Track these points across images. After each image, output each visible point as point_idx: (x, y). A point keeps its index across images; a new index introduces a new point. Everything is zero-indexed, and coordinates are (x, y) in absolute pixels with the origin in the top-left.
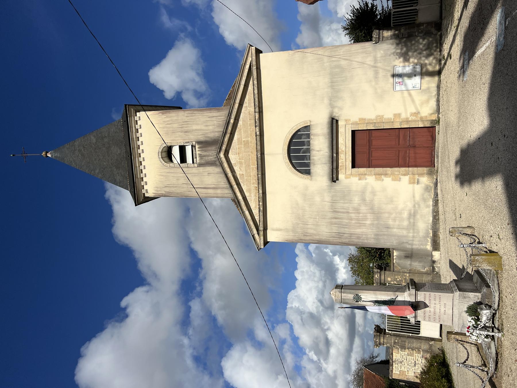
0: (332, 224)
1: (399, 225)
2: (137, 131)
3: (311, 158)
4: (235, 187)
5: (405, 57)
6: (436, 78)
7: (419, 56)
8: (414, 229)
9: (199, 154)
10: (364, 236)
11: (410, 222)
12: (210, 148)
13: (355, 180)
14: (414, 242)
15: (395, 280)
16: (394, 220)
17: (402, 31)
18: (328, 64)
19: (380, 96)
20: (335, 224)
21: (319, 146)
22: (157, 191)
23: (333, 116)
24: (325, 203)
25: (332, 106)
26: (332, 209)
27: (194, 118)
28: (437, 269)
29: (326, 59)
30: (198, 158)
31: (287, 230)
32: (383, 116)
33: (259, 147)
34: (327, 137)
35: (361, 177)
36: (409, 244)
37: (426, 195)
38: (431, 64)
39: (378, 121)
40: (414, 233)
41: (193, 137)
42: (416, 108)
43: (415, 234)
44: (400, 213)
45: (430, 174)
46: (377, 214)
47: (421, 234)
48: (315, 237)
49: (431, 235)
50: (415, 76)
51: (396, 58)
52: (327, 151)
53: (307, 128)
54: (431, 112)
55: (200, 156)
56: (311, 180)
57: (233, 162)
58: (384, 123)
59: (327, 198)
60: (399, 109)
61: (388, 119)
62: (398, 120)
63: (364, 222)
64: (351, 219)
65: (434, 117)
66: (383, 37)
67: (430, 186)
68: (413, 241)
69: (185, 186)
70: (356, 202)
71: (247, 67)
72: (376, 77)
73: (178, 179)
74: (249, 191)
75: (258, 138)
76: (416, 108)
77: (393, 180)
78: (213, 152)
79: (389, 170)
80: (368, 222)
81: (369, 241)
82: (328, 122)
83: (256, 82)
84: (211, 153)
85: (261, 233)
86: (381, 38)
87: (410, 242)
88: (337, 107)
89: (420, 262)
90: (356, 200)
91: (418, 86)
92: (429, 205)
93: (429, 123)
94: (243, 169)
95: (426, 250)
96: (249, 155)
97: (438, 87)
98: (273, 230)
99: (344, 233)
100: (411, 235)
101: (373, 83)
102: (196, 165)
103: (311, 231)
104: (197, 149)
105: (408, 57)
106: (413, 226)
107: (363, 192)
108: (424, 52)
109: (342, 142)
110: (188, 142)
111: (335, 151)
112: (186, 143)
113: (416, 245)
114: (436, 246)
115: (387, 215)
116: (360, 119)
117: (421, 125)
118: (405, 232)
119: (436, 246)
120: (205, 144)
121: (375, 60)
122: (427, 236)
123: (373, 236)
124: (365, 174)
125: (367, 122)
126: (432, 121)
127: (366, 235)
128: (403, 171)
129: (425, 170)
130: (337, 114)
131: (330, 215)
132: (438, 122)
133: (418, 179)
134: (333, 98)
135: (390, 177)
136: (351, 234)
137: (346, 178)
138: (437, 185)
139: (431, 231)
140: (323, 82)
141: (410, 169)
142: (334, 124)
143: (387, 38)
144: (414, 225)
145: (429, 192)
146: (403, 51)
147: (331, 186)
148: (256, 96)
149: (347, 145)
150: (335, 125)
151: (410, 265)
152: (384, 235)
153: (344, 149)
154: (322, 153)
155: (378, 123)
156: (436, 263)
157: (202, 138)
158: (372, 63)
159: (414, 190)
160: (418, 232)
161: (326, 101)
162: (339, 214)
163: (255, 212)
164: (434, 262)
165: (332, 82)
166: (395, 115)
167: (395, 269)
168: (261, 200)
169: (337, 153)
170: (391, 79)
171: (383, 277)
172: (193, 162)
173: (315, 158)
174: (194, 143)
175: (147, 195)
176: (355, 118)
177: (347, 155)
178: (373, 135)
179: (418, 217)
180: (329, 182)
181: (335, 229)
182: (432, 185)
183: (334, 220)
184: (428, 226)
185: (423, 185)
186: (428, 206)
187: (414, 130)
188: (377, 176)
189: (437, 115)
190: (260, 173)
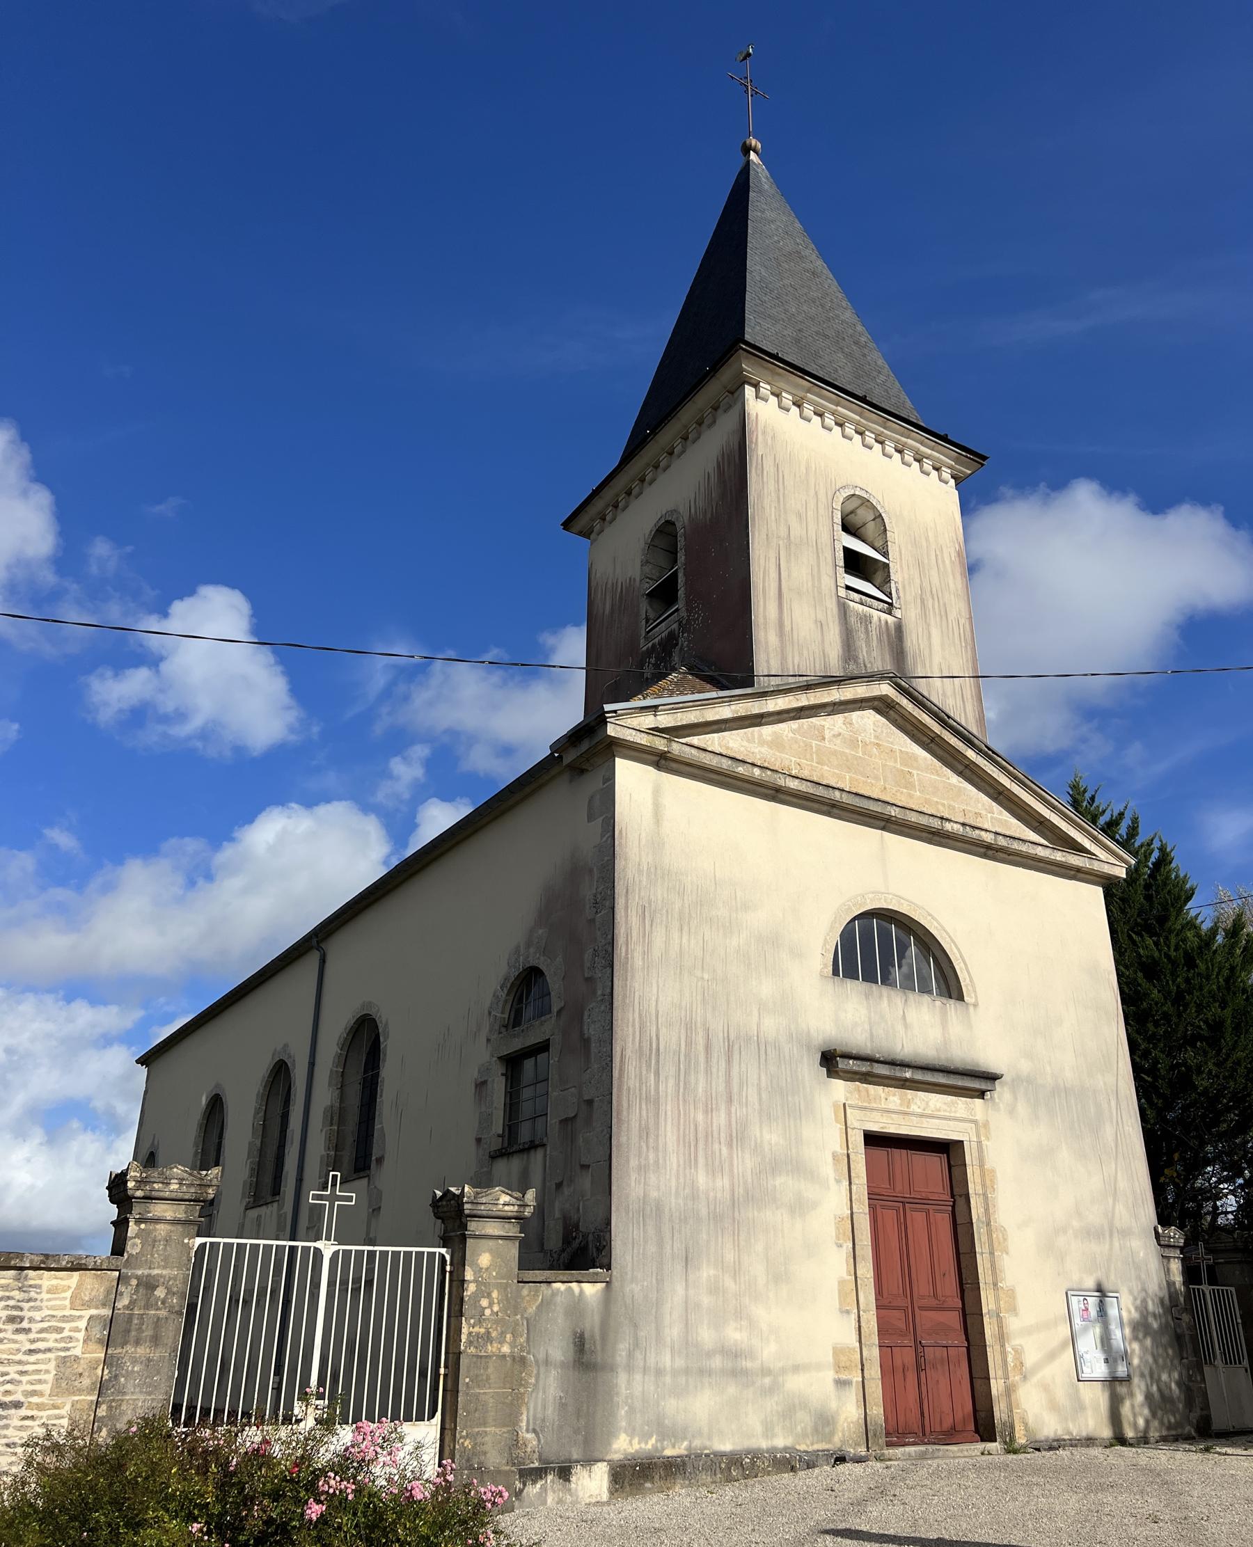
0: (689, 1027)
4: (803, 700)
5: (1140, 1328)
6: (1106, 1433)
7: (1147, 1372)
8: (687, 1371)
10: (651, 1156)
11: (710, 1354)
12: (888, 657)
14: (638, 1377)
15: (484, 1291)
16: (715, 1289)
20: (689, 1044)
21: (909, 1023)
24: (755, 1013)
26: (738, 1038)
27: (957, 641)
28: (533, 1490)
31: (657, 844)
36: (630, 1355)
37: (804, 1420)
38: (1136, 1413)
40: (675, 1373)
42: (1038, 1367)
43: (668, 1379)
44: (740, 1314)
46: (732, 1215)
47: (671, 1406)
49: (669, 1452)
50: (1106, 1361)
51: (1135, 1299)
52: (906, 1050)
54: (1031, 1420)
57: (856, 716)
59: (771, 1026)
63: (701, 1161)
64: (708, 1111)
67: (832, 1433)
68: (645, 1370)
69: (783, 532)
70: (767, 1136)
71: (1087, 844)
73: (799, 515)
74: (777, 743)
76: (1038, 1367)
78: (879, 663)
79: (866, 1270)
80: (702, 1179)
81: (634, 1176)
85: (660, 744)
89: (562, 1406)
90: (771, 1137)
91: (1087, 1373)
92: (774, 1436)
93: (1005, 1417)
94: (837, 745)
95: (611, 1435)
97: (1089, 1441)
99: (657, 1074)
100: (667, 1360)
101: (1075, 1224)
104: (884, 616)
105: (1141, 1335)
106: (698, 1369)
107: (799, 1168)
108: (1155, 1388)
111: (919, 1076)
114: (632, 1476)
115: (730, 1257)
118: (673, 1332)
119: (632, 1476)
121: (1125, 1233)
122: (667, 1432)
123: (654, 1194)
127: (657, 1162)
132: (1011, 1449)
143: (1168, 1271)
144: (703, 1372)
145: (816, 1430)
146: (1151, 1320)
147: (809, 1048)
151: (547, 1362)
152: (660, 1244)
154: (900, 1028)
156: (559, 1483)
158: (1117, 1223)
162: (723, 1064)
163: (733, 742)
164: (564, 1473)
167: (526, 1290)
168: (767, 776)
170: (1090, 1283)
171: (493, 1228)
178: (939, 1215)
179: (732, 1390)
180: (820, 1037)
181: (670, 1038)
183: (701, 1041)
184: (700, 1433)
185: (833, 1405)
186: (768, 1431)
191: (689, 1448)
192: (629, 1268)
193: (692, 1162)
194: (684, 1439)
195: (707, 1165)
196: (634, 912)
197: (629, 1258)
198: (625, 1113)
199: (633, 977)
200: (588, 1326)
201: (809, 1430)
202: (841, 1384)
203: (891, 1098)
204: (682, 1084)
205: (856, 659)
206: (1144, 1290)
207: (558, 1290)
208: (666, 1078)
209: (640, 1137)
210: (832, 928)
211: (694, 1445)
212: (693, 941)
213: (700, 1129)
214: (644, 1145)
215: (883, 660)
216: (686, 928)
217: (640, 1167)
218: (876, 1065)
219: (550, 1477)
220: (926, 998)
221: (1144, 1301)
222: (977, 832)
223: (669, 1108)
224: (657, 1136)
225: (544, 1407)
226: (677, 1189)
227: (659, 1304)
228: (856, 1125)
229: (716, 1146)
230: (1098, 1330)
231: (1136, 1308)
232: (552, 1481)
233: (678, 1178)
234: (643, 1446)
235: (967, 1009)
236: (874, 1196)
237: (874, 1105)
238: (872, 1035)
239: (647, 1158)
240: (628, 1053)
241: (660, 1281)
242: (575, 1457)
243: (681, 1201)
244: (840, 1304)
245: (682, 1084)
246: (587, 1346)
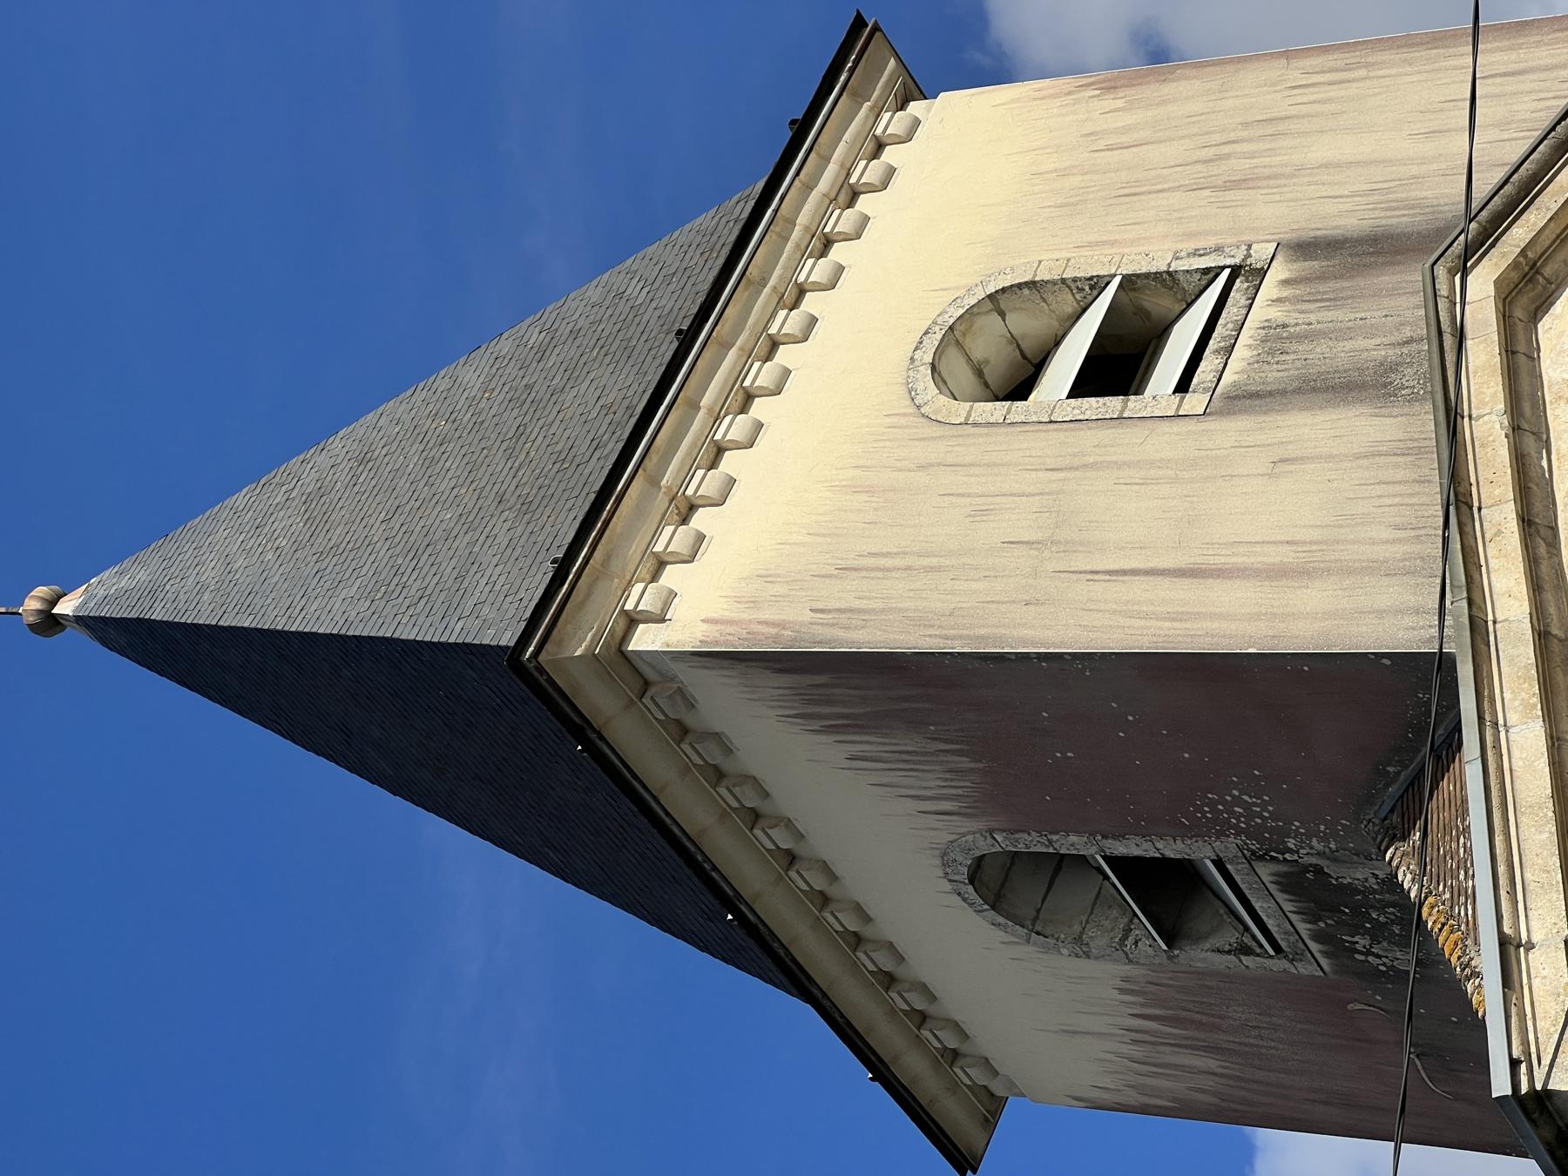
12: (1386, 279)
27: (1353, 90)
57: (1552, 369)
78: (1404, 302)
104: (1269, 288)
157: (1343, 214)
215: (1392, 293)
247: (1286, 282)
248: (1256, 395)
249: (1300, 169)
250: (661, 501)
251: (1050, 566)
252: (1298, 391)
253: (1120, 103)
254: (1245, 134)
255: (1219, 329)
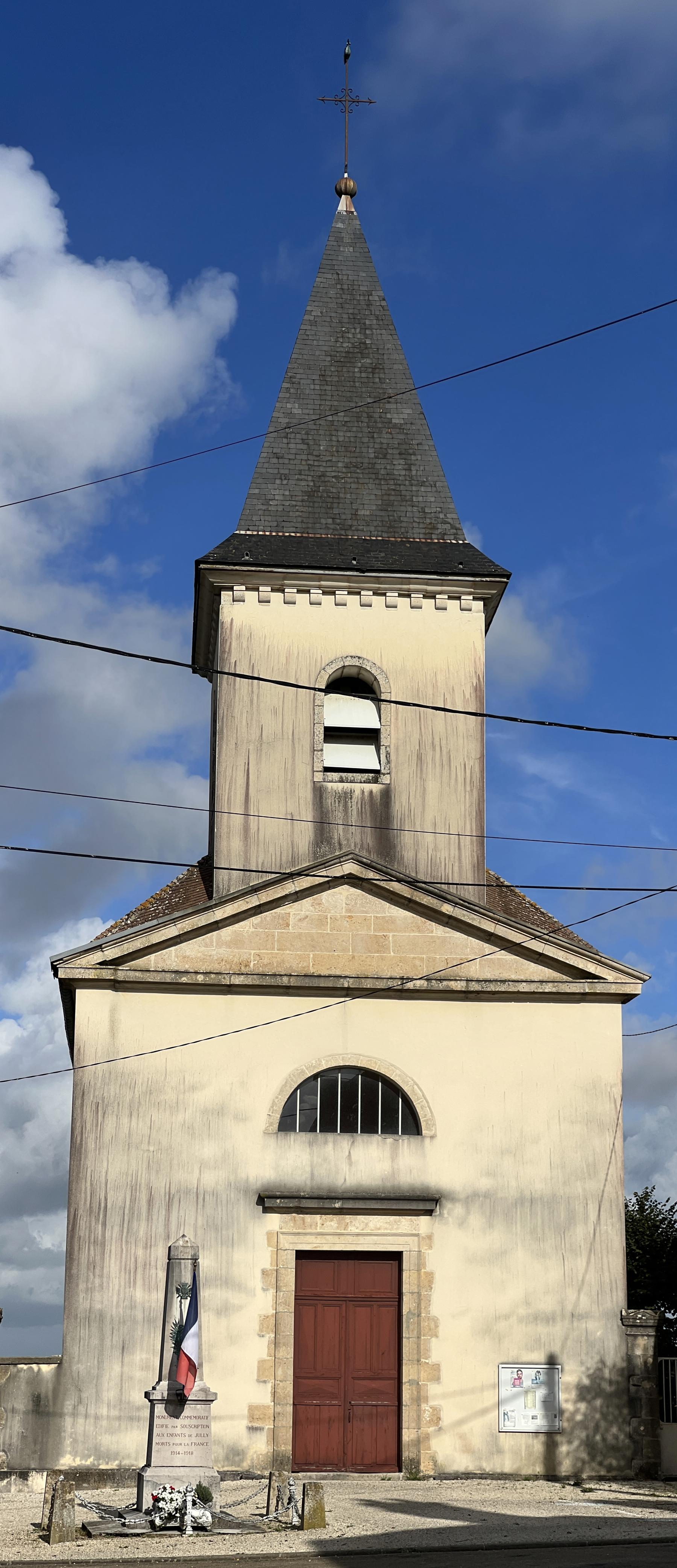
0: (134, 1188)
1: (131, 1378)
2: (431, 596)
3: (330, 1136)
4: (254, 901)
5: (584, 1393)
8: (119, 1418)
9: (352, 792)
10: (97, 1281)
13: (264, 1258)
14: (81, 1420)
17: (647, 1385)
18: (580, 1190)
19: (489, 1329)
20: (133, 1200)
21: (365, 1160)
22: (239, 637)
23: (444, 1201)
24: (197, 1171)
25: (472, 1198)
26: (178, 1191)
27: (460, 787)
29: (593, 1186)
30: (341, 785)
32: (437, 1337)
33: (368, 984)
34: (389, 1184)
35: (272, 1277)
39: (424, 1324)
41: (402, 777)
43: (104, 1423)
45: (277, 1461)
48: (92, 1136)
49: (102, 1467)
52: (348, 1183)
53: (413, 1125)
54: (440, 1459)
55: (346, 796)
56: (266, 1133)
57: (326, 896)
58: (419, 1338)
59: (210, 1179)
60: (450, 1380)
61: (428, 1350)
62: (423, 1375)
63: (139, 1282)
65: (426, 1468)
66: (635, 1336)
67: (242, 1461)
68: (86, 1416)
69: (255, 733)
71: (591, 968)
72: (536, 1318)
74: (237, 942)
75: (396, 984)
77: (261, 1363)
79: (288, 1353)
80: (139, 1294)
81: (82, 1295)
82: (428, 1188)
83: (548, 988)
84: (353, 834)
86: (634, 1331)
87: (82, 1409)
88: (468, 1212)
89: (23, 1437)
91: (509, 1426)
93: (412, 1455)
95: (59, 1454)
96: (345, 950)
98: (113, 1011)
99: (104, 1224)
100: (104, 1411)
101: (522, 1311)
102: (319, 777)
103: (110, 1125)
104: (368, 787)
109: (371, 1225)
110: (389, 762)
111: (350, 1205)
112: (388, 754)
113: (73, 1425)
116: (430, 1276)
117: (407, 1435)
118: (110, 1393)
120: (382, 814)
123: (98, 1306)
124: (277, 1289)
125: (423, 1293)
126: (416, 1463)
127: (101, 1286)
128: (284, 1388)
129: (287, 1448)
130: (450, 1211)
131: (160, 1185)
133: (261, 1429)
134: (489, 1203)
135: (269, 1355)
136: (103, 1244)
137: (269, 1234)
138: (247, 1478)
139: (113, 1465)
140: (535, 1175)
141: (290, 1409)
142: (423, 1202)
143: (630, 1348)
145: (227, 1458)
147: (246, 1191)
148: (512, 988)
149: (361, 1239)
150: (421, 1206)
151: (13, 1410)
152: (102, 1339)
153: (352, 1229)
154: (344, 1167)
155: (419, 1324)
156: (19, 1481)
157: (399, 806)
159: (232, 1418)
160: (111, 1431)
161: (484, 1184)
162: (163, 1212)
164: (24, 1475)
165: (532, 1201)
166: (437, 1367)
168: (212, 979)
169: (341, 1212)
172: (327, 770)
173: (330, 1146)
174: (386, 779)
175: (225, 596)
176: (434, 1261)
177: (336, 1239)
180: (259, 1184)
181: (116, 1198)
182: (245, 1466)
183: (143, 1197)
184: (129, 1456)
185: (244, 1443)
187: (393, 1419)
188: (272, 1321)
189: (432, 1473)
190: (293, 982)
191: (120, 1465)
192: (77, 1353)
193: (131, 1283)
194: (115, 1460)
195: (144, 1284)
196: (89, 1109)
197: (76, 1349)
198: (76, 1253)
199: (86, 1157)
200: (43, 1391)
201: (221, 1458)
202: (252, 1429)
203: (328, 1223)
204: (125, 1230)
205: (329, 841)
206: (603, 1362)
207: (22, 1369)
208: (112, 1227)
209: (88, 1269)
210: (281, 1091)
211: (123, 1463)
212: (140, 1125)
213: (139, 1260)
214: (91, 1275)
216: (135, 1114)
217: (87, 1289)
218: (304, 1201)
219: (13, 1477)
220: (376, 1139)
221: (599, 1370)
222: (445, 983)
223: (113, 1248)
224: (103, 1268)
225: (11, 1437)
226: (118, 1302)
227: (99, 1377)
228: (287, 1246)
229: (153, 1271)
230: (541, 1393)
231: (589, 1376)
232: (15, 1479)
233: (119, 1294)
234: (83, 1462)
235: (423, 1141)
236: (300, 1299)
237: (309, 1231)
238: (312, 1174)
239: (93, 1282)
240: (80, 1212)
241: (100, 1362)
242: (33, 1466)
243: (121, 1310)
244: (258, 1376)
245: (125, 1230)
246: (42, 1403)
247: (371, 792)
248: (321, 797)
249: (423, 780)
250: (280, 582)
251: (251, 748)
252: (322, 812)
253: (468, 696)
254: (444, 753)
255: (350, 775)
